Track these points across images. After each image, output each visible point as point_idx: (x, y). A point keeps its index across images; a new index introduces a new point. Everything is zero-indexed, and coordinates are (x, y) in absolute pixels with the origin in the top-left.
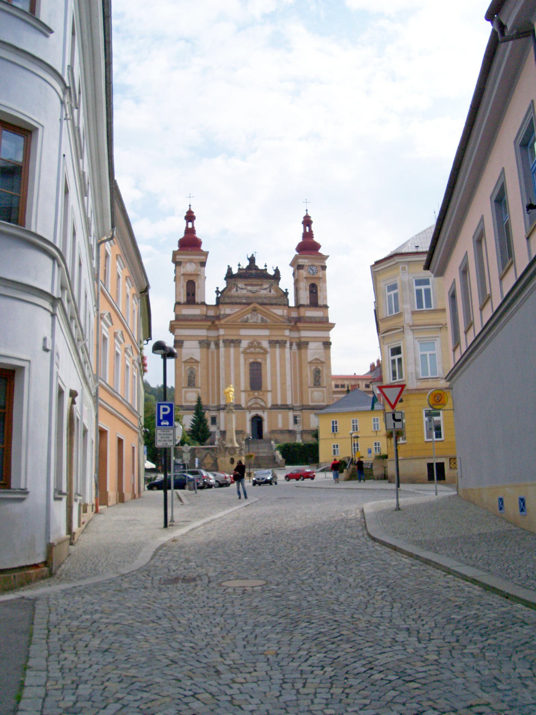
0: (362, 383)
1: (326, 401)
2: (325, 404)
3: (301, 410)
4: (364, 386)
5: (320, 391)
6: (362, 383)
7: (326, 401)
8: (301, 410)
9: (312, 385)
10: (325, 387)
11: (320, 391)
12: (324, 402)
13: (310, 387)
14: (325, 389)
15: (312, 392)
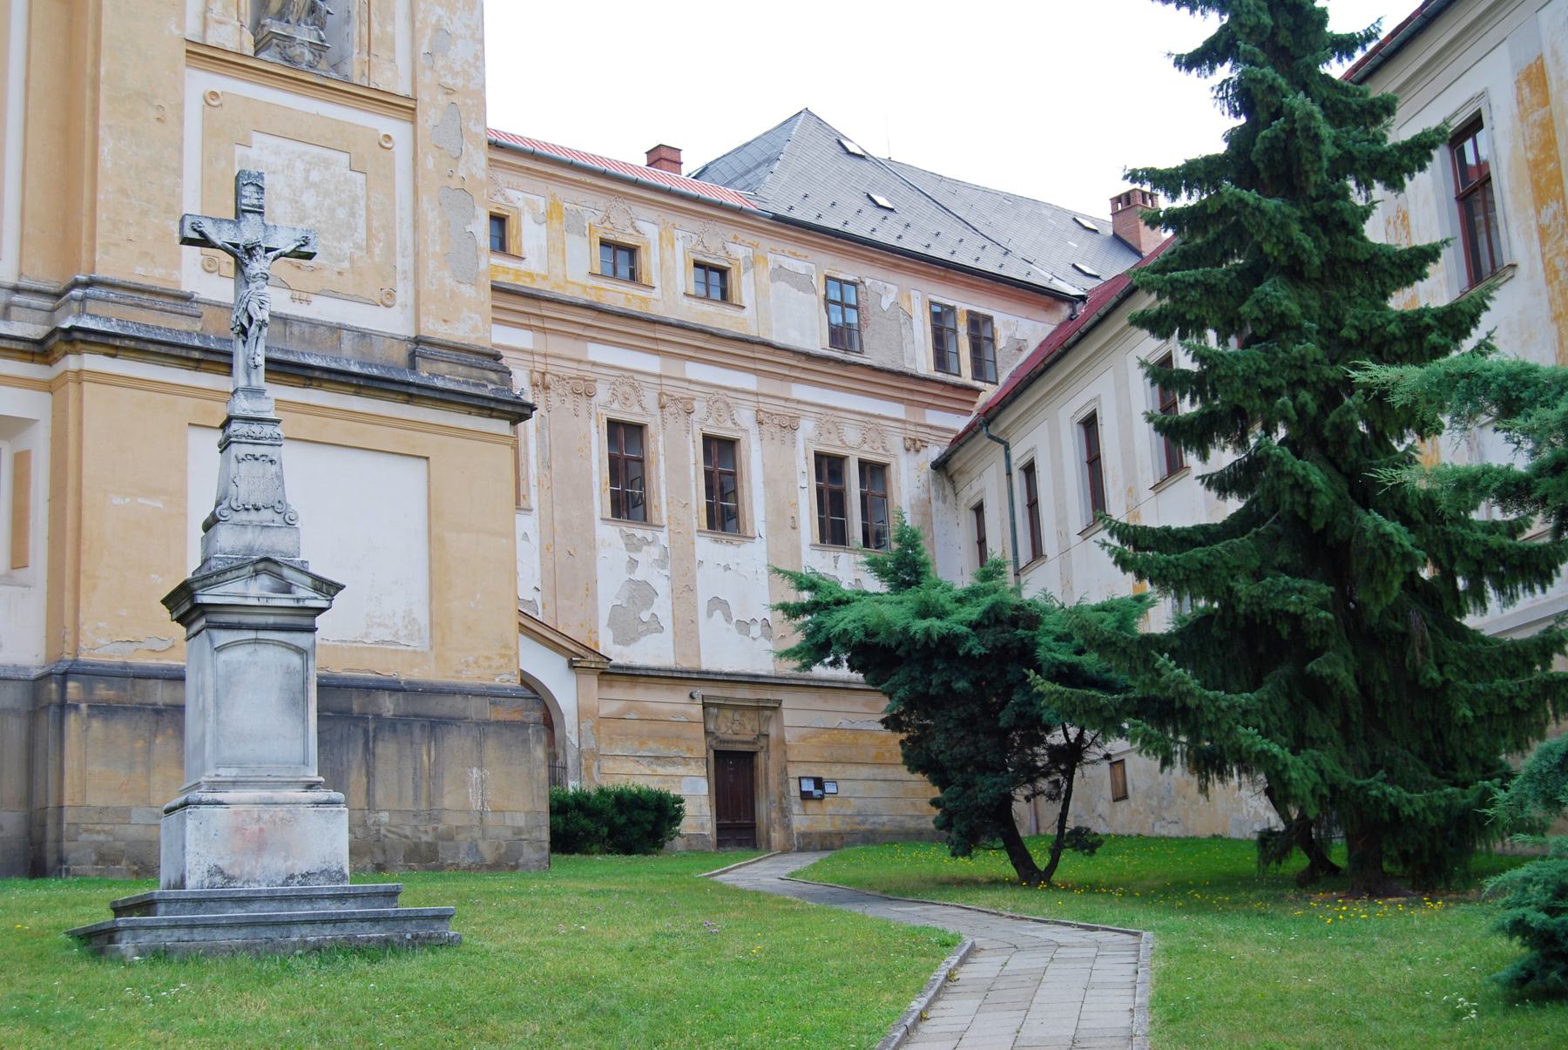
0: (666, 241)
1: (404, 293)
2: (394, 322)
3: (39, 351)
4: (684, 278)
5: (336, 139)
6: (666, 241)
7: (404, 293)
8: (39, 351)
9: (233, 36)
10: (406, 108)
11: (336, 139)
12: (387, 300)
13: (202, 55)
14: (396, 128)
15: (223, 126)
